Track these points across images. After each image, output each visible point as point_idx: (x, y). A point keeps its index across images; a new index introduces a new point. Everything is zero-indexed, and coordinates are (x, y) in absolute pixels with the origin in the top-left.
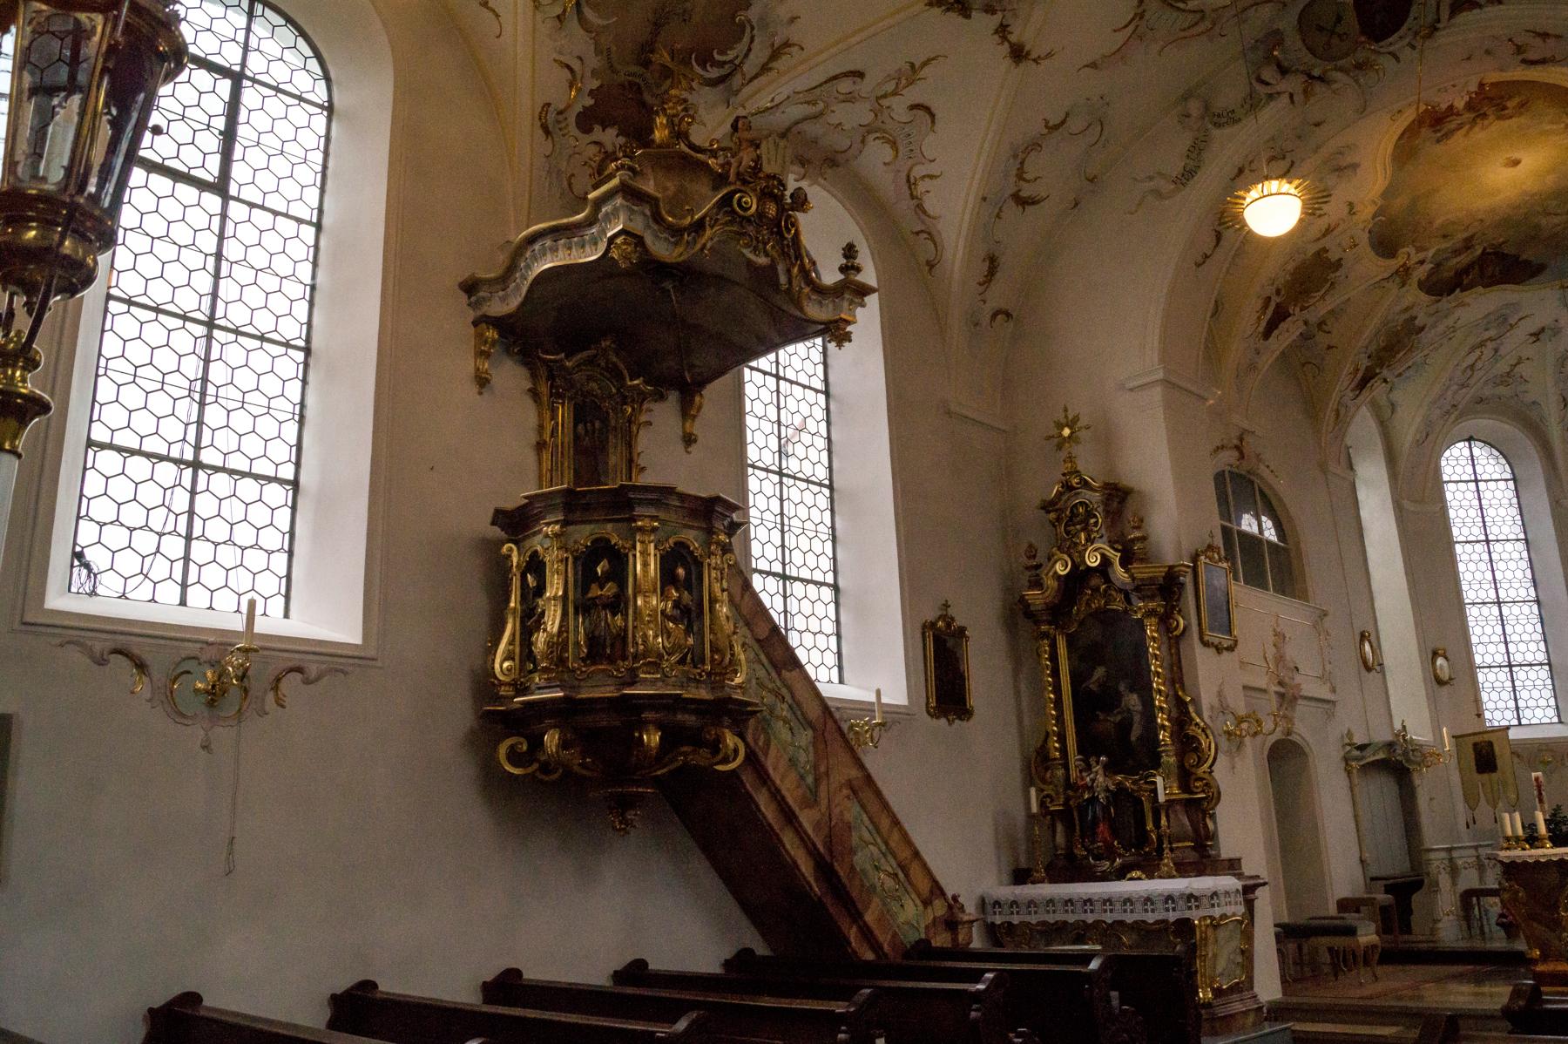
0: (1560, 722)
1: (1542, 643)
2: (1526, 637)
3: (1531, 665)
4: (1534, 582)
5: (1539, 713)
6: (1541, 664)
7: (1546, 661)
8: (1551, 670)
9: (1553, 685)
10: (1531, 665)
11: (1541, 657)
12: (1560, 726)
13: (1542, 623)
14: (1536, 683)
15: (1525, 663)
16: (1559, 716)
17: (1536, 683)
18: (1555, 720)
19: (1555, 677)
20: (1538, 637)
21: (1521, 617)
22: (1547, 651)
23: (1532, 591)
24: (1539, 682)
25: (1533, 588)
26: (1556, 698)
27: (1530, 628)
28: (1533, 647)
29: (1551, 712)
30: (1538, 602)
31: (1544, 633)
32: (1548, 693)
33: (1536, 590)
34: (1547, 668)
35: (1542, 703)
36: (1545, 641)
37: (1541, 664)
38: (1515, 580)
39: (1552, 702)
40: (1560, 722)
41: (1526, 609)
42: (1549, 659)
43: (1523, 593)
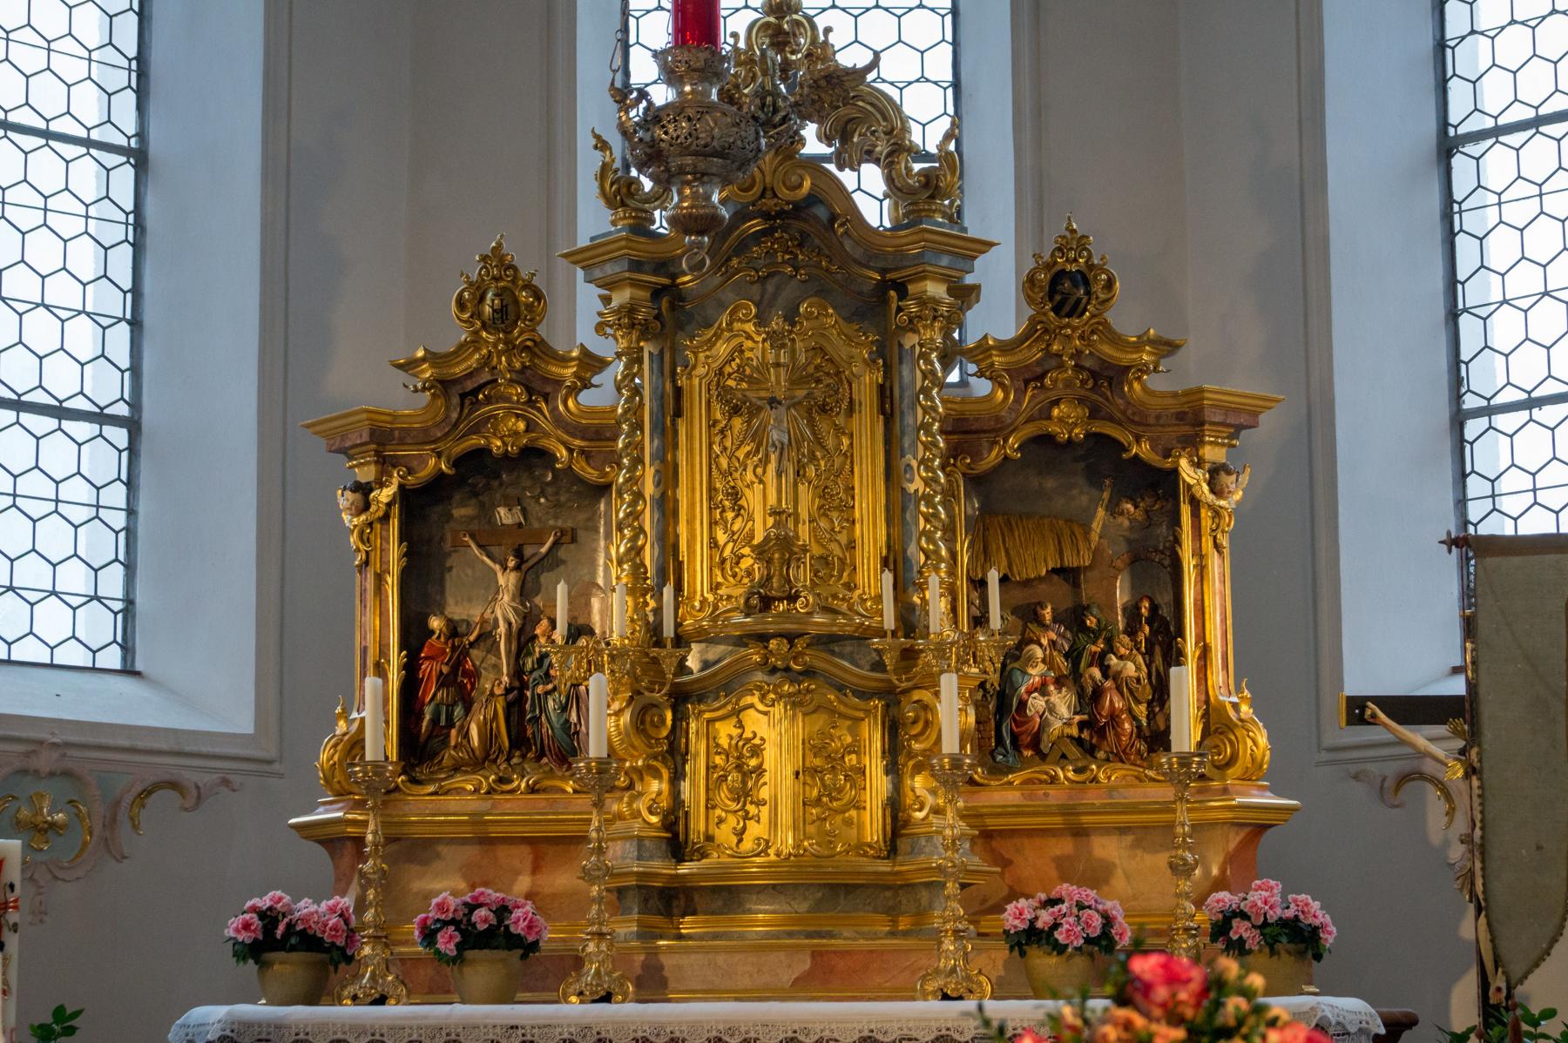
0: (128, 671)
1: (124, 329)
2: (63, 292)
3: (59, 412)
4: (142, 74)
5: (53, 620)
6: (100, 417)
7: (122, 410)
8: (133, 449)
9: (131, 512)
10: (59, 412)
11: (108, 388)
12: (125, 685)
13: (138, 248)
14: (66, 492)
15: (39, 397)
16: (127, 649)
17: (66, 492)
18: (112, 658)
19: (144, 479)
20: (114, 303)
21: (63, 202)
22: (135, 369)
23: (126, 109)
24: (77, 490)
25: (130, 97)
26: (130, 568)
27: (85, 259)
28: (83, 337)
29: (100, 625)
30: (139, 157)
31: (136, 291)
32: (102, 544)
33: (141, 107)
34: (120, 436)
35: (74, 579)
36: (136, 324)
37: (100, 417)
38: (68, 45)
39: (113, 583)
40: (128, 671)
41: (86, 174)
42: (135, 404)
43: (89, 106)
